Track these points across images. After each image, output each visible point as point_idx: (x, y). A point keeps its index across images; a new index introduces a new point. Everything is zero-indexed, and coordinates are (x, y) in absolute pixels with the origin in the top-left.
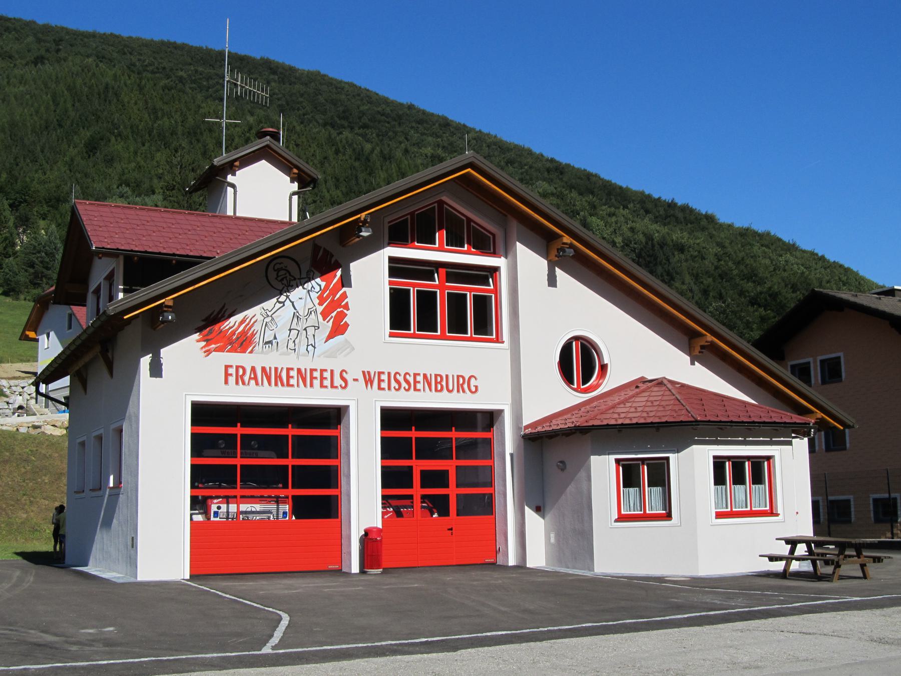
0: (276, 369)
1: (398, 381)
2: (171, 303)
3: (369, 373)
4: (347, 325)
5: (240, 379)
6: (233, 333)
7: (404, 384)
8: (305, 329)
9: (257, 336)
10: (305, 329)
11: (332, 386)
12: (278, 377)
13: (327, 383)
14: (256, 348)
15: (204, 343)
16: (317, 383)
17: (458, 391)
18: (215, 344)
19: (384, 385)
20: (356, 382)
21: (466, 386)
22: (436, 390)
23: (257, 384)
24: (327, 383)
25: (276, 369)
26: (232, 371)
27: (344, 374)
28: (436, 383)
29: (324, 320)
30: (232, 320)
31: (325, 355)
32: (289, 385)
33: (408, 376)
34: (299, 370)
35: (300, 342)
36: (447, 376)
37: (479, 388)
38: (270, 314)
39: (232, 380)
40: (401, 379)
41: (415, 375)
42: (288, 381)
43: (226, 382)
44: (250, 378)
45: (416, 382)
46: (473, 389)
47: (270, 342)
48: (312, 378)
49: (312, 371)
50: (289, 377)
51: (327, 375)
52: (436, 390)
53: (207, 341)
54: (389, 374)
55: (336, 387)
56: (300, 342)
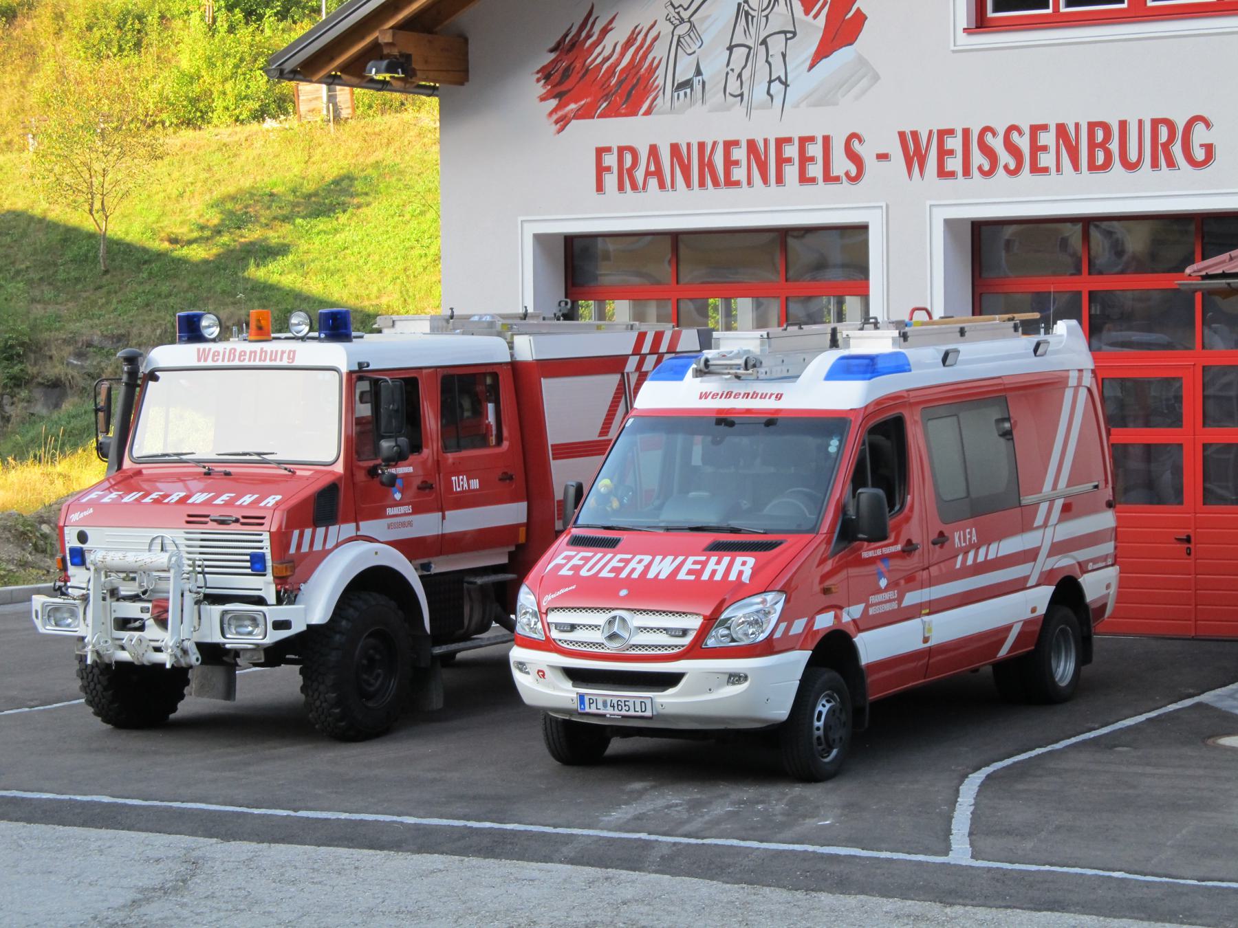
0: (702, 146)
1: (988, 151)
2: (387, 38)
3: (915, 134)
4: (860, 18)
5: (627, 180)
6: (611, 71)
7: (1005, 158)
8: (764, 42)
9: (660, 72)
10: (764, 42)
11: (829, 178)
12: (707, 165)
13: (815, 170)
14: (659, 101)
15: (553, 103)
16: (791, 172)
17: (1155, 164)
18: (576, 102)
19: (954, 164)
20: (884, 164)
21: (1177, 149)
22: (1092, 167)
23: (662, 186)
24: (815, 170)
25: (702, 146)
26: (610, 160)
27: (856, 144)
28: (1092, 146)
29: (807, 12)
30: (609, 41)
31: (811, 99)
32: (731, 183)
33: (1015, 136)
34: (752, 145)
35: (753, 75)
36: (1123, 125)
37: (1218, 152)
38: (685, 15)
39: (611, 180)
40: (997, 144)
41: (1035, 130)
42: (727, 173)
43: (600, 188)
44: (648, 174)
45: (1036, 149)
46: (1199, 155)
47: (687, 84)
48: (781, 161)
49: (781, 142)
50: (729, 163)
51: (815, 150)
52: (1092, 167)
53: (559, 95)
54: (966, 132)
55: (837, 179)
56: (753, 75)
